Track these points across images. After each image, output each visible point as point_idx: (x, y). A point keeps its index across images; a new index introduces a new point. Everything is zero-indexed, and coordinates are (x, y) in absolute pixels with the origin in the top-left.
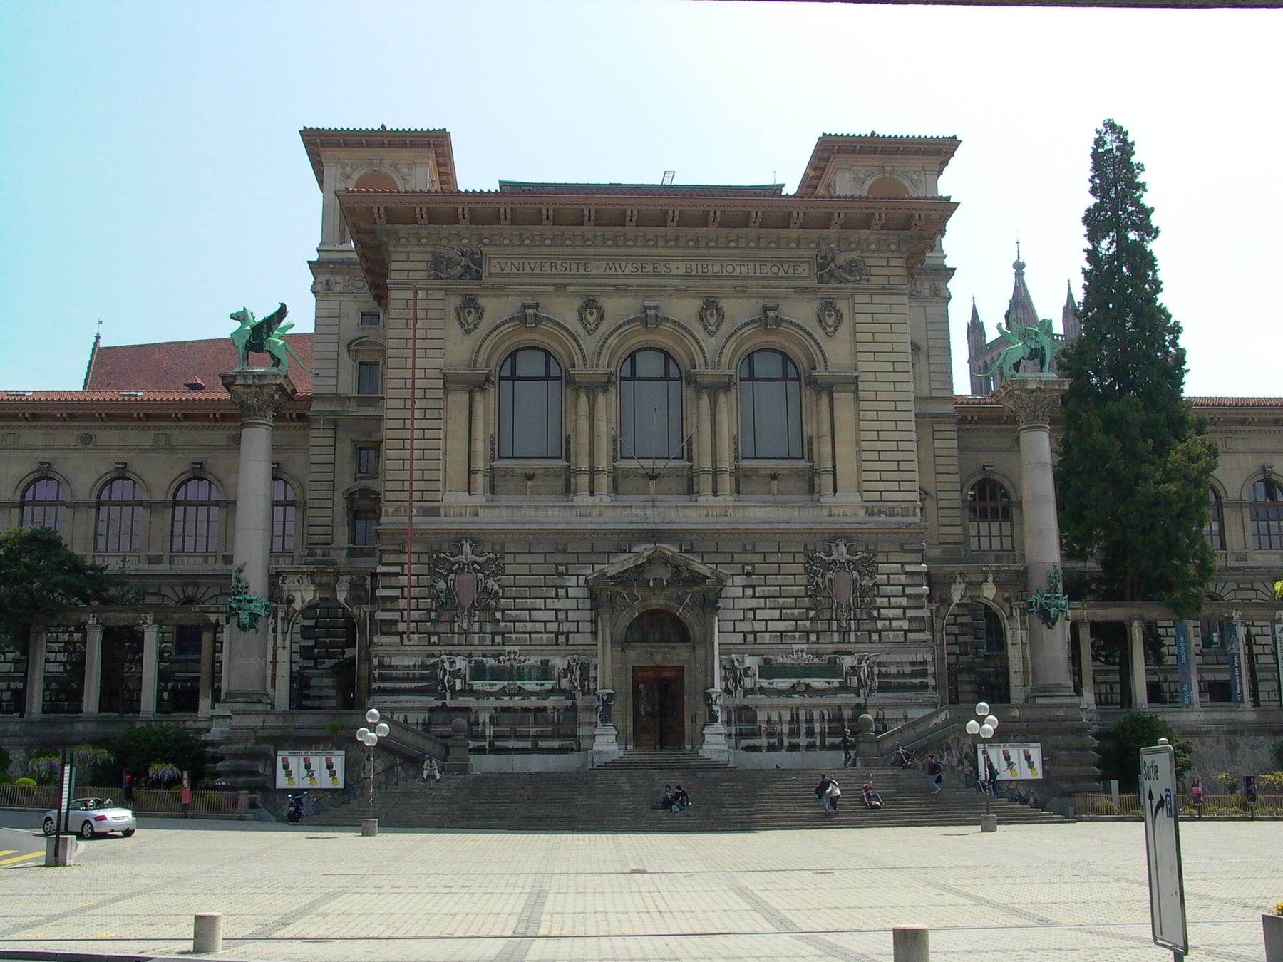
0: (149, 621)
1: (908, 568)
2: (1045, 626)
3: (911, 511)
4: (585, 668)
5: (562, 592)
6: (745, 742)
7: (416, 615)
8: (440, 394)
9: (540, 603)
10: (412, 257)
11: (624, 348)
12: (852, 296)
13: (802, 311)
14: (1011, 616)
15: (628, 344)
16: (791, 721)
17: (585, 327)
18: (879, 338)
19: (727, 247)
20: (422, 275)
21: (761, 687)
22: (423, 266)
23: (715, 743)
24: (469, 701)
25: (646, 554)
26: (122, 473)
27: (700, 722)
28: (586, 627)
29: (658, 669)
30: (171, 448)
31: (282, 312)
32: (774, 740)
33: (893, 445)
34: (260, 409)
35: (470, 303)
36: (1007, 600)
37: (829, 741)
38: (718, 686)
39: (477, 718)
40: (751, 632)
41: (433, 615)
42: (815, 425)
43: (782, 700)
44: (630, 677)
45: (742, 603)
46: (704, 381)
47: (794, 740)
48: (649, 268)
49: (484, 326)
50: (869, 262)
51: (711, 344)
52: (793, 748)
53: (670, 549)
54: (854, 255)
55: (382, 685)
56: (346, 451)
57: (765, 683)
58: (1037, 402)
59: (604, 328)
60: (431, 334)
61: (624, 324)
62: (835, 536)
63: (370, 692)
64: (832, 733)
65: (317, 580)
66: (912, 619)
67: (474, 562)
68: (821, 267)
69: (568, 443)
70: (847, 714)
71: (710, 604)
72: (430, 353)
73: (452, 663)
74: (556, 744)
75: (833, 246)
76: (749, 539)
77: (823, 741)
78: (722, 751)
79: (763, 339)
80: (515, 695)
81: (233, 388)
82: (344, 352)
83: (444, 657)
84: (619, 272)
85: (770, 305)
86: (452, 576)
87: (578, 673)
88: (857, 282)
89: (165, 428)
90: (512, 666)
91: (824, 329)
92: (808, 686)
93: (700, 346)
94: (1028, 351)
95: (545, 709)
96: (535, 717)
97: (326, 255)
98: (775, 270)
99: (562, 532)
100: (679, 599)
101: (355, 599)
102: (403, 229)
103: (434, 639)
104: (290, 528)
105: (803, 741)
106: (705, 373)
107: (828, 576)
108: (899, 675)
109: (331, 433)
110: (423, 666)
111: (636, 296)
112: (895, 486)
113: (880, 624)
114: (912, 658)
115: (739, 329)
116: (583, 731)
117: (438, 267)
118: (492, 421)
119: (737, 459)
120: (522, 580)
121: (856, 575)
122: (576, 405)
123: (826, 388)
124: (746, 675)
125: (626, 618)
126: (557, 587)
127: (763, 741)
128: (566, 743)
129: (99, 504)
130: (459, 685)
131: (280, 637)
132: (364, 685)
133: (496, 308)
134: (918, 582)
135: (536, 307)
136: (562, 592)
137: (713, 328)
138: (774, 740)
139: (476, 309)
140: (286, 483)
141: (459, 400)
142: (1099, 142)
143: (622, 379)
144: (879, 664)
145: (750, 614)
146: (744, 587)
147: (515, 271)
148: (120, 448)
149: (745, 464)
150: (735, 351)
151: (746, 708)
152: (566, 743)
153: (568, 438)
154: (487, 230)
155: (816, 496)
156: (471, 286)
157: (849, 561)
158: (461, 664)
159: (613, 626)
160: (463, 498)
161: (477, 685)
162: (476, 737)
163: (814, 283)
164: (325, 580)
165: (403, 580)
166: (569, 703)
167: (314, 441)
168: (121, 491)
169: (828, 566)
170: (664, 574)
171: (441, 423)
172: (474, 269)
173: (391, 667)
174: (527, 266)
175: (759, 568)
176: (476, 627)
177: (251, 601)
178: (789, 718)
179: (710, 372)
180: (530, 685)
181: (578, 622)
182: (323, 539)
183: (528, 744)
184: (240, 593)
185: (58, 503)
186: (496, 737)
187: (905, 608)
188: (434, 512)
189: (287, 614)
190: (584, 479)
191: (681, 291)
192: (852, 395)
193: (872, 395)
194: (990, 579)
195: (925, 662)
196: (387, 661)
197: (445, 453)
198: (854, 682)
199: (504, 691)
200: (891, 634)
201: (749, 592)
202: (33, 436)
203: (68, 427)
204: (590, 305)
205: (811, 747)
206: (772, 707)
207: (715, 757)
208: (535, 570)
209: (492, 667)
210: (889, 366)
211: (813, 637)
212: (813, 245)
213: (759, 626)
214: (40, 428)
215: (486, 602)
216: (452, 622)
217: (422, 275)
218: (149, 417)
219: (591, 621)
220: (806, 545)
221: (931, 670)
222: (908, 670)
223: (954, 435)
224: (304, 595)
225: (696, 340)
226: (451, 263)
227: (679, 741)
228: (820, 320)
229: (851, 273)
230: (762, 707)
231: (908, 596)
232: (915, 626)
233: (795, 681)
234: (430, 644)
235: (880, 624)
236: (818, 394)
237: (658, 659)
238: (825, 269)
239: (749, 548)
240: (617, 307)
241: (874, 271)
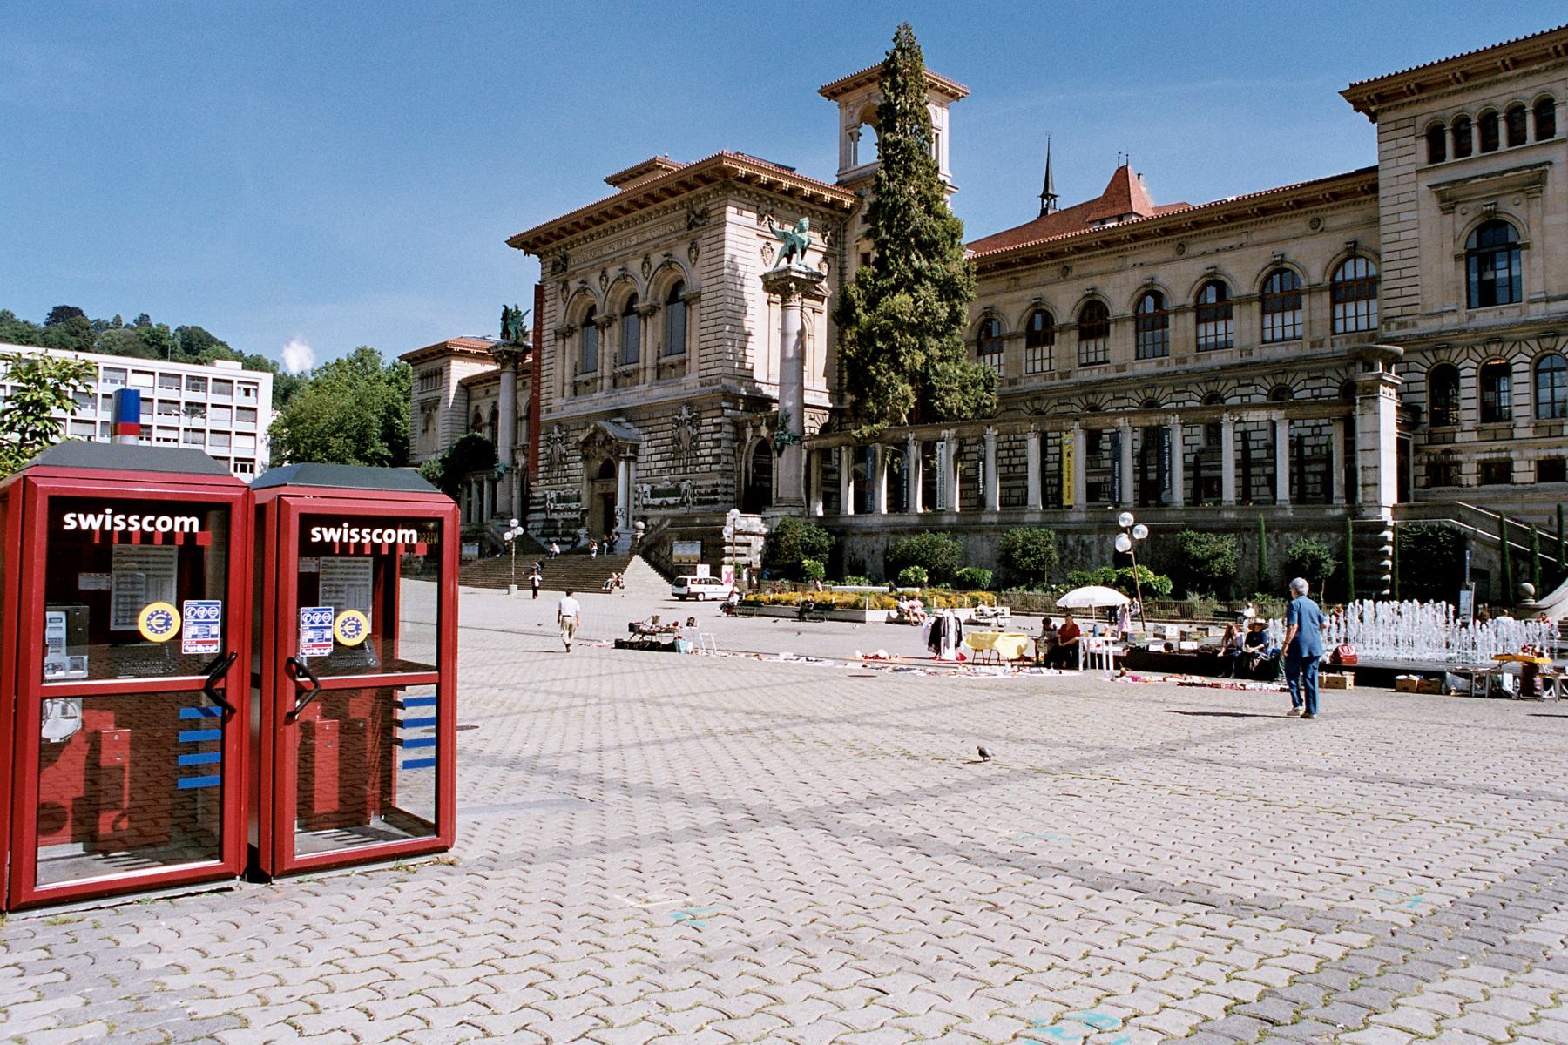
21: (653, 507)
24: (555, 515)
54: (702, 205)
57: (651, 501)
62: (689, 403)
66: (714, 456)
99: (587, 416)
133: (574, 285)
149: (663, 360)
161: (559, 506)
162: (556, 535)
180: (573, 506)
188: (549, 411)
191: (634, 254)
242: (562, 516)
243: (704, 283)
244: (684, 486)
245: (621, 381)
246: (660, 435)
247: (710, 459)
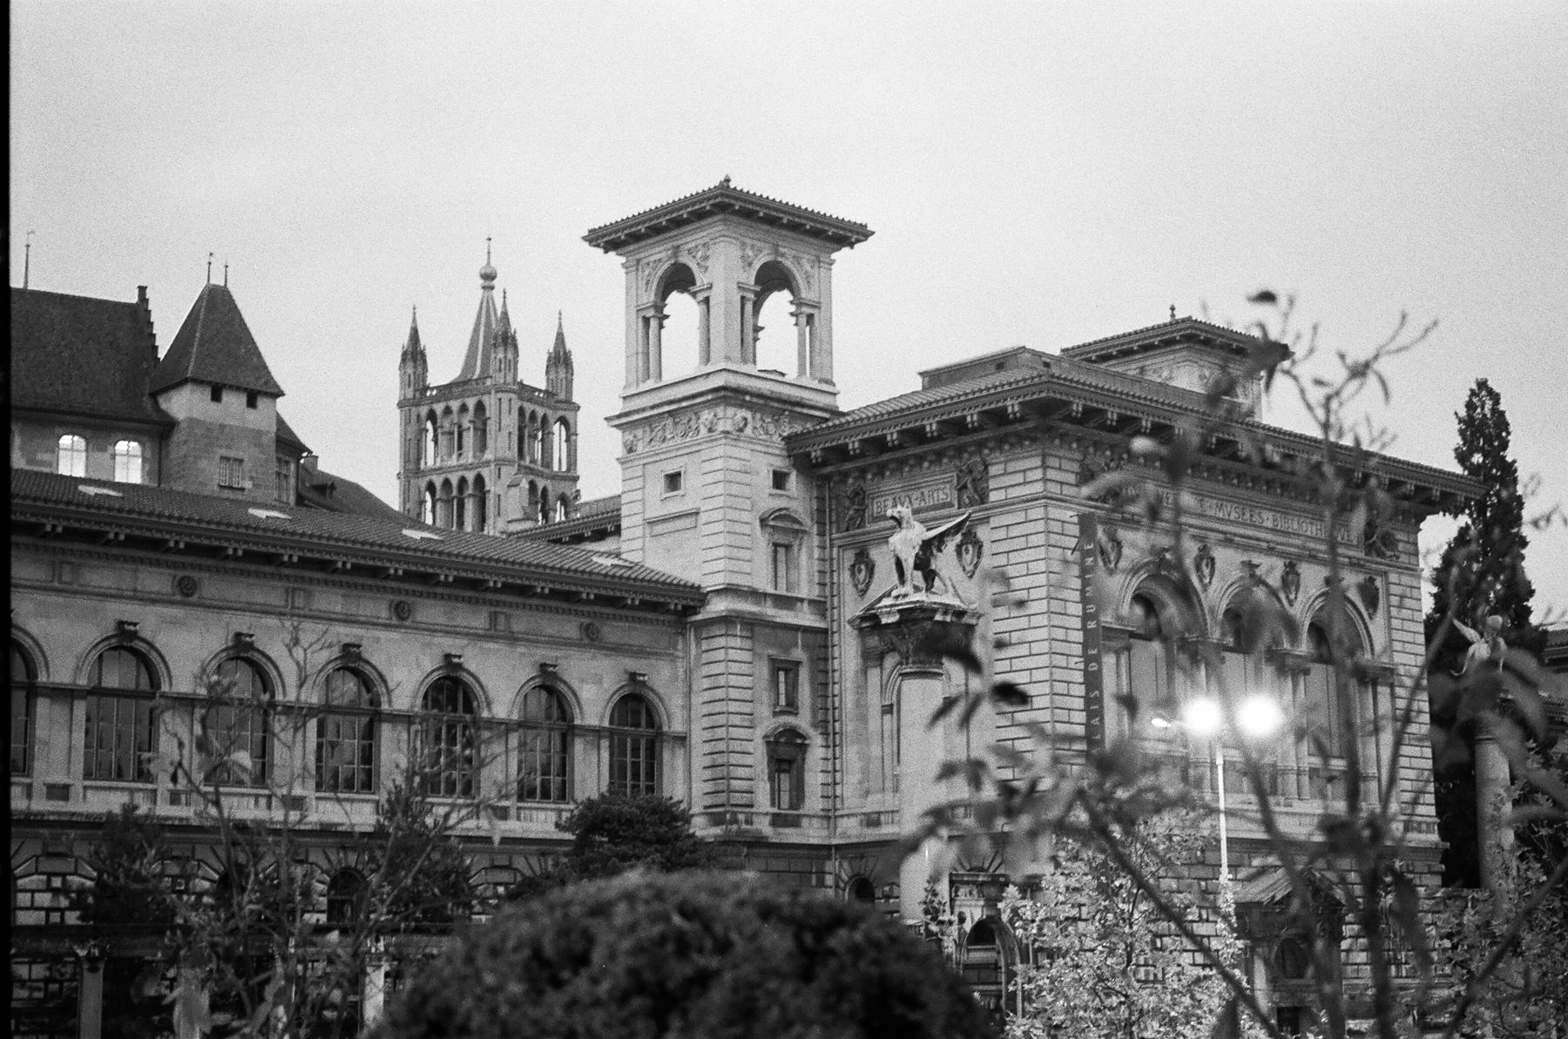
30: (512, 639)
89: (505, 604)
111: (1238, 546)
163: (1361, 555)
191: (1270, 551)
243: (1398, 658)
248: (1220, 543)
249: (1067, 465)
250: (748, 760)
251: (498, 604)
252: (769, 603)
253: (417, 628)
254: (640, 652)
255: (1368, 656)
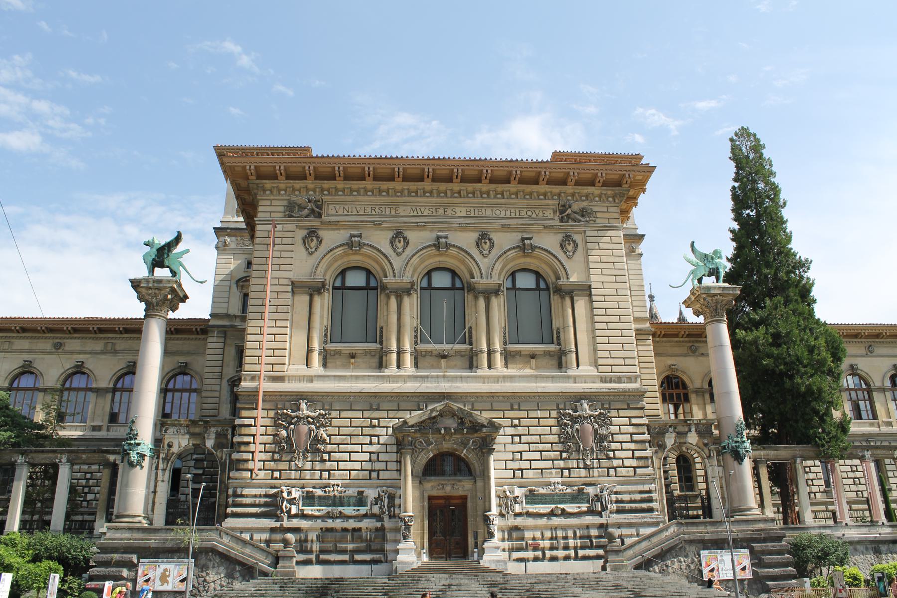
0: (63, 461)
1: (634, 421)
2: (735, 463)
3: (633, 379)
4: (392, 498)
5: (375, 439)
6: (516, 555)
7: (263, 456)
8: (289, 295)
9: (358, 448)
10: (274, 203)
11: (422, 266)
12: (584, 231)
13: (549, 241)
14: (709, 457)
15: (427, 263)
16: (551, 538)
17: (395, 250)
18: (604, 259)
19: (496, 198)
20: (281, 215)
21: (529, 514)
22: (281, 209)
23: (495, 554)
25: (438, 409)
26: (79, 370)
27: (480, 540)
28: (393, 466)
29: (448, 498)
30: (115, 353)
31: (178, 239)
32: (539, 554)
33: (618, 333)
34: (158, 305)
35: (312, 233)
36: (706, 445)
37: (581, 553)
38: (495, 510)
39: (307, 536)
40: (519, 470)
41: (276, 457)
42: (561, 320)
43: (543, 521)
44: (426, 504)
45: (511, 448)
46: (481, 288)
47: (554, 553)
48: (441, 211)
49: (323, 249)
50: (595, 209)
51: (484, 263)
52: (553, 559)
53: (456, 406)
55: (235, 510)
56: (231, 352)
57: (532, 509)
58: (717, 303)
59: (409, 251)
60: (284, 254)
61: (423, 248)
62: (579, 397)
63: (227, 516)
64: (582, 548)
65: (192, 430)
67: (308, 417)
68: (561, 212)
69: (381, 332)
70: (594, 532)
71: (486, 447)
72: (282, 268)
73: (289, 493)
74: (368, 557)
75: (569, 198)
76: (515, 401)
77: (576, 553)
78: (498, 561)
79: (523, 262)
80: (337, 518)
81: (139, 289)
82: (234, 286)
83: (284, 488)
84: (420, 214)
85: (526, 235)
86: (292, 426)
87: (386, 501)
88: (587, 222)
89: (112, 338)
90: (335, 496)
91: (565, 253)
92: (563, 510)
93: (477, 264)
94: (707, 270)
95: (360, 529)
96: (353, 535)
97: (225, 225)
98: (529, 213)
100: (465, 444)
101: (219, 446)
102: (268, 184)
103: (276, 474)
104: (193, 406)
105: (561, 553)
106: (480, 281)
107: (577, 426)
108: (631, 501)
109: (222, 340)
110: (266, 496)
111: (432, 230)
112: (621, 361)
113: (616, 463)
114: (641, 488)
115: (505, 252)
116: (388, 547)
117: (291, 210)
118: (326, 316)
119: (505, 343)
120: (344, 430)
121: (596, 426)
122: (387, 304)
123: (569, 293)
124: (516, 502)
125: (424, 458)
126: (371, 436)
127: (530, 554)
128: (376, 556)
129: (61, 391)
130: (294, 510)
131: (160, 473)
132: (222, 512)
133: (331, 238)
134: (641, 431)
135: (360, 236)
136: (375, 439)
137: (487, 252)
138: (539, 554)
139: (318, 237)
140: (192, 376)
141: (303, 299)
142: (735, 149)
143: (421, 288)
144: (616, 493)
145: (518, 456)
146: (513, 435)
147: (346, 212)
148: (80, 352)
150: (502, 269)
151: (516, 528)
152: (376, 556)
153: (382, 328)
154: (327, 184)
155: (563, 369)
156: (314, 222)
157: (590, 416)
158: (296, 494)
159: (413, 465)
160: (303, 370)
161: (308, 510)
163: (558, 222)
164: (197, 430)
165: (253, 430)
166: (379, 525)
167: (209, 346)
168: (78, 381)
169: (574, 420)
170: (452, 423)
171: (289, 316)
172: (317, 213)
173: (242, 496)
174: (354, 209)
175: (524, 422)
176: (309, 465)
177: (138, 444)
178: (549, 535)
179: (485, 281)
180: (349, 511)
181: (386, 462)
182: (212, 412)
183: (346, 557)
184: (131, 438)
185: (35, 389)
186: (322, 551)
187: (633, 451)
188: (280, 379)
189: (167, 455)
190: (394, 356)
191: (463, 227)
192: (587, 298)
193: (602, 298)
194: (693, 429)
195: (650, 492)
196: (239, 491)
197: (290, 338)
198: (599, 507)
199: (328, 516)
200: (623, 471)
201: (517, 439)
202: (23, 344)
203: (46, 338)
204: (398, 234)
205: (567, 558)
206: (535, 528)
207: (493, 567)
208: (356, 422)
209: (320, 497)
210: (613, 278)
211: (566, 473)
212: (555, 197)
213: (525, 465)
214: (28, 338)
215: (315, 447)
216: (290, 461)
217: (281, 215)
218: (101, 331)
219: (397, 462)
220: (558, 405)
221: (655, 496)
222: (638, 497)
223: (651, 342)
224: (180, 441)
225: (474, 260)
226: (301, 208)
227: (464, 554)
228: (562, 246)
229: (583, 216)
230: (529, 528)
231: (636, 442)
232: (641, 463)
233: (553, 506)
234: (272, 478)
235: (616, 463)
236: (563, 298)
237: (448, 489)
238: (564, 213)
239: (516, 407)
240: (418, 238)
241: (598, 215)
242: (319, 524)
244: (590, 490)
245: (420, 360)
246: (539, 430)
247: (634, 463)
248: (412, 229)
249: (278, 203)
250: (217, 394)
251: (108, 338)
252: (238, 320)
253: (65, 352)
254: (189, 353)
255: (565, 279)
